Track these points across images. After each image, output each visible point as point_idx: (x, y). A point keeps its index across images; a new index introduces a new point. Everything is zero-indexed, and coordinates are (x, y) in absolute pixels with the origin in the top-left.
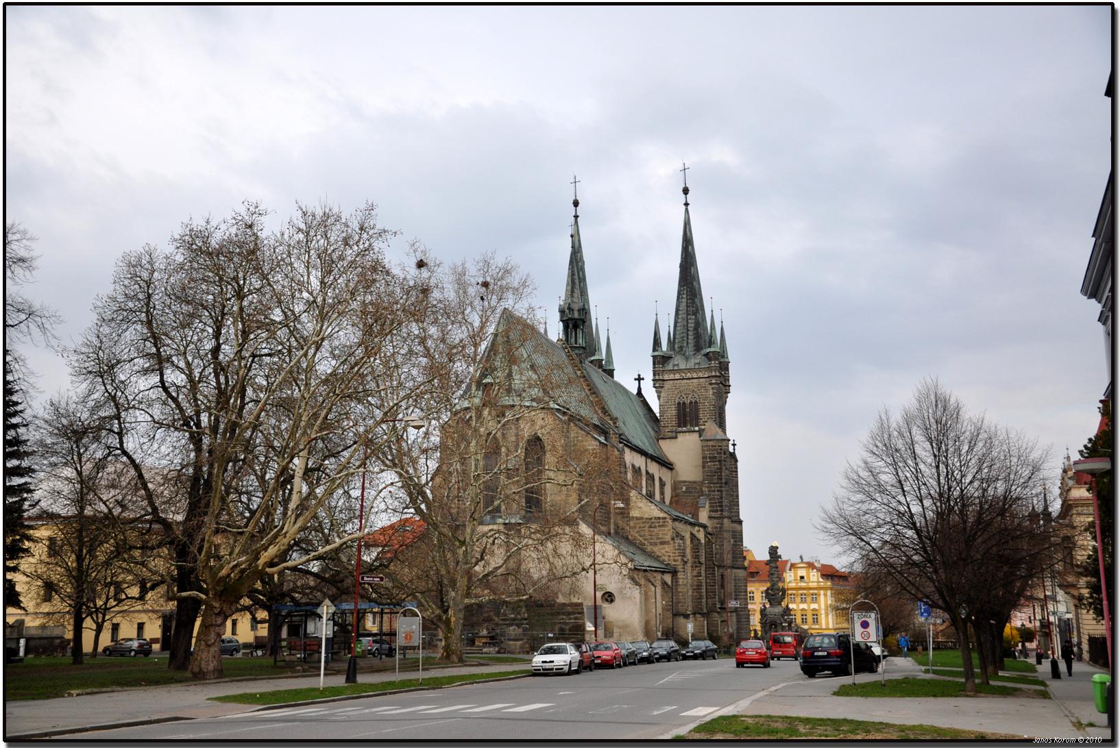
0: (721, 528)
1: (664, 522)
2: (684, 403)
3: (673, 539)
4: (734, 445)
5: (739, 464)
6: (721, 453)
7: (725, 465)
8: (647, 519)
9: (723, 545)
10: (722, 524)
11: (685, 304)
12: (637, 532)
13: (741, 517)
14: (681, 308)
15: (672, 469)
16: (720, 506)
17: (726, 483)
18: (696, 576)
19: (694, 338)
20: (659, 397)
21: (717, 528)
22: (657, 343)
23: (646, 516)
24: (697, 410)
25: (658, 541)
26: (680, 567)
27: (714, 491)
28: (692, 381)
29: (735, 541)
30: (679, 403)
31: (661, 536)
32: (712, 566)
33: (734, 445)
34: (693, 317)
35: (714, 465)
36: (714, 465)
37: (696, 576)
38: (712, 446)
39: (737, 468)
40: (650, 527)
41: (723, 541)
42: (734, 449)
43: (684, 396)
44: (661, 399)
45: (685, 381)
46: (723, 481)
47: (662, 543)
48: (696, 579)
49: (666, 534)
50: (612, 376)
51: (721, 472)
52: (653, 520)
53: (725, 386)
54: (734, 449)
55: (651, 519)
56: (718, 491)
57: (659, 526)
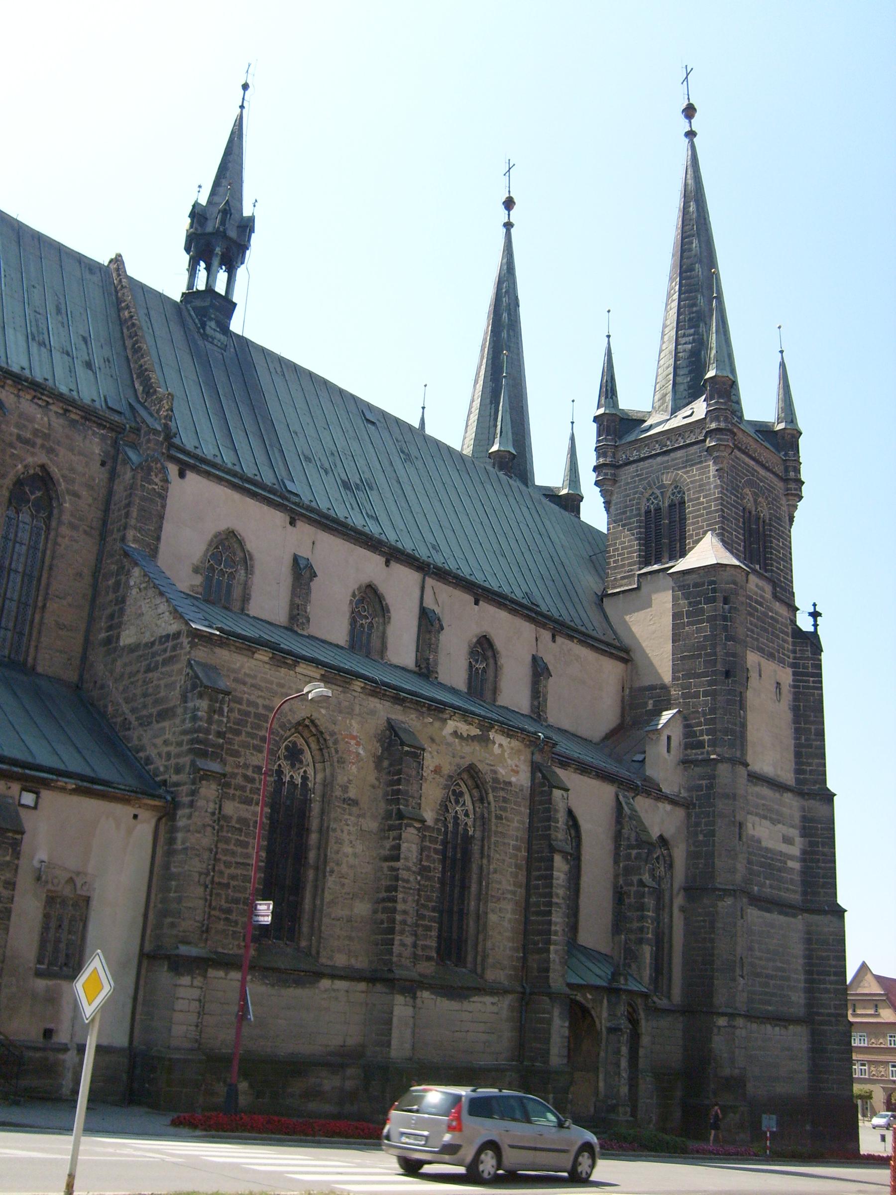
0: (710, 787)
1: (174, 648)
2: (658, 510)
3: (184, 699)
4: (815, 615)
5: (824, 656)
6: (713, 600)
7: (725, 628)
8: (146, 645)
9: (712, 833)
10: (713, 777)
11: (675, 310)
12: (125, 690)
13: (831, 785)
14: (668, 322)
15: (625, 661)
16: (708, 732)
17: (727, 674)
18: (386, 859)
19: (690, 372)
20: (608, 505)
21: (699, 788)
22: (609, 390)
23: (147, 638)
24: (683, 519)
25: (154, 711)
26: (184, 789)
27: (696, 695)
28: (672, 455)
29: (811, 844)
30: (648, 512)
31: (163, 694)
32: (546, 854)
33: (815, 615)
34: (692, 331)
35: (698, 630)
36: (698, 630)
37: (386, 859)
38: (696, 585)
39: (819, 667)
40: (149, 670)
41: (713, 823)
42: (816, 625)
43: (658, 492)
44: (613, 508)
45: (659, 459)
46: (720, 667)
47: (164, 715)
48: (386, 865)
49: (170, 686)
50: (576, 510)
51: (714, 646)
52: (156, 647)
53: (786, 480)
54: (816, 625)
55: (153, 643)
56: (706, 694)
57: (165, 662)
